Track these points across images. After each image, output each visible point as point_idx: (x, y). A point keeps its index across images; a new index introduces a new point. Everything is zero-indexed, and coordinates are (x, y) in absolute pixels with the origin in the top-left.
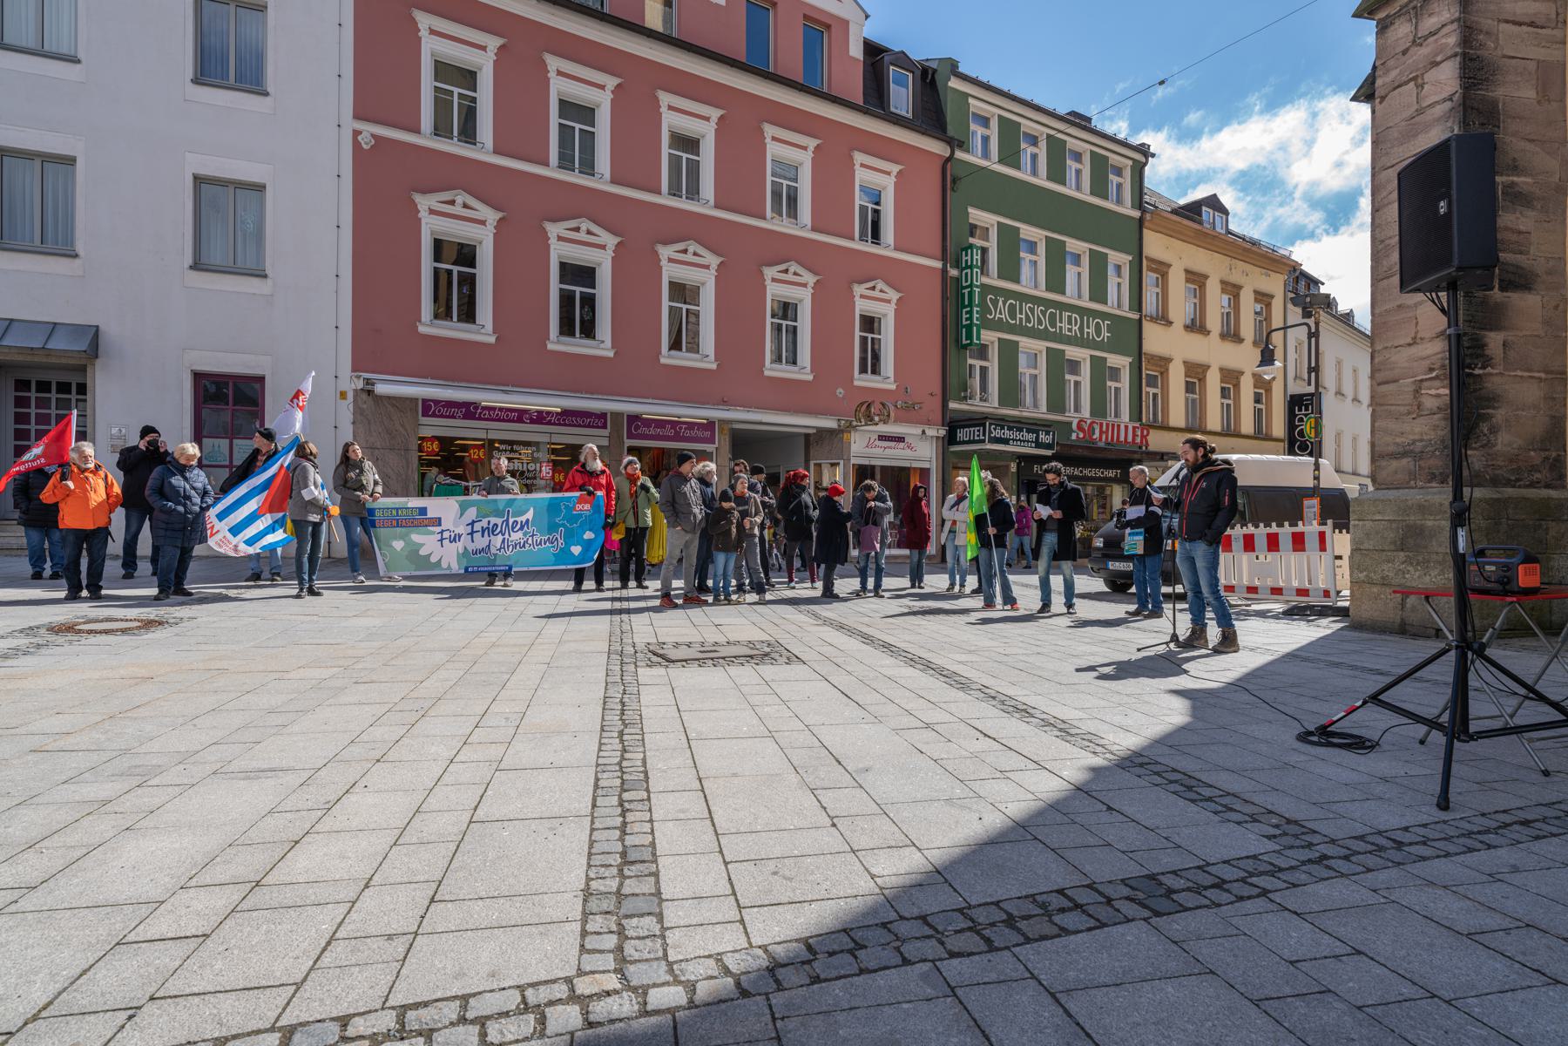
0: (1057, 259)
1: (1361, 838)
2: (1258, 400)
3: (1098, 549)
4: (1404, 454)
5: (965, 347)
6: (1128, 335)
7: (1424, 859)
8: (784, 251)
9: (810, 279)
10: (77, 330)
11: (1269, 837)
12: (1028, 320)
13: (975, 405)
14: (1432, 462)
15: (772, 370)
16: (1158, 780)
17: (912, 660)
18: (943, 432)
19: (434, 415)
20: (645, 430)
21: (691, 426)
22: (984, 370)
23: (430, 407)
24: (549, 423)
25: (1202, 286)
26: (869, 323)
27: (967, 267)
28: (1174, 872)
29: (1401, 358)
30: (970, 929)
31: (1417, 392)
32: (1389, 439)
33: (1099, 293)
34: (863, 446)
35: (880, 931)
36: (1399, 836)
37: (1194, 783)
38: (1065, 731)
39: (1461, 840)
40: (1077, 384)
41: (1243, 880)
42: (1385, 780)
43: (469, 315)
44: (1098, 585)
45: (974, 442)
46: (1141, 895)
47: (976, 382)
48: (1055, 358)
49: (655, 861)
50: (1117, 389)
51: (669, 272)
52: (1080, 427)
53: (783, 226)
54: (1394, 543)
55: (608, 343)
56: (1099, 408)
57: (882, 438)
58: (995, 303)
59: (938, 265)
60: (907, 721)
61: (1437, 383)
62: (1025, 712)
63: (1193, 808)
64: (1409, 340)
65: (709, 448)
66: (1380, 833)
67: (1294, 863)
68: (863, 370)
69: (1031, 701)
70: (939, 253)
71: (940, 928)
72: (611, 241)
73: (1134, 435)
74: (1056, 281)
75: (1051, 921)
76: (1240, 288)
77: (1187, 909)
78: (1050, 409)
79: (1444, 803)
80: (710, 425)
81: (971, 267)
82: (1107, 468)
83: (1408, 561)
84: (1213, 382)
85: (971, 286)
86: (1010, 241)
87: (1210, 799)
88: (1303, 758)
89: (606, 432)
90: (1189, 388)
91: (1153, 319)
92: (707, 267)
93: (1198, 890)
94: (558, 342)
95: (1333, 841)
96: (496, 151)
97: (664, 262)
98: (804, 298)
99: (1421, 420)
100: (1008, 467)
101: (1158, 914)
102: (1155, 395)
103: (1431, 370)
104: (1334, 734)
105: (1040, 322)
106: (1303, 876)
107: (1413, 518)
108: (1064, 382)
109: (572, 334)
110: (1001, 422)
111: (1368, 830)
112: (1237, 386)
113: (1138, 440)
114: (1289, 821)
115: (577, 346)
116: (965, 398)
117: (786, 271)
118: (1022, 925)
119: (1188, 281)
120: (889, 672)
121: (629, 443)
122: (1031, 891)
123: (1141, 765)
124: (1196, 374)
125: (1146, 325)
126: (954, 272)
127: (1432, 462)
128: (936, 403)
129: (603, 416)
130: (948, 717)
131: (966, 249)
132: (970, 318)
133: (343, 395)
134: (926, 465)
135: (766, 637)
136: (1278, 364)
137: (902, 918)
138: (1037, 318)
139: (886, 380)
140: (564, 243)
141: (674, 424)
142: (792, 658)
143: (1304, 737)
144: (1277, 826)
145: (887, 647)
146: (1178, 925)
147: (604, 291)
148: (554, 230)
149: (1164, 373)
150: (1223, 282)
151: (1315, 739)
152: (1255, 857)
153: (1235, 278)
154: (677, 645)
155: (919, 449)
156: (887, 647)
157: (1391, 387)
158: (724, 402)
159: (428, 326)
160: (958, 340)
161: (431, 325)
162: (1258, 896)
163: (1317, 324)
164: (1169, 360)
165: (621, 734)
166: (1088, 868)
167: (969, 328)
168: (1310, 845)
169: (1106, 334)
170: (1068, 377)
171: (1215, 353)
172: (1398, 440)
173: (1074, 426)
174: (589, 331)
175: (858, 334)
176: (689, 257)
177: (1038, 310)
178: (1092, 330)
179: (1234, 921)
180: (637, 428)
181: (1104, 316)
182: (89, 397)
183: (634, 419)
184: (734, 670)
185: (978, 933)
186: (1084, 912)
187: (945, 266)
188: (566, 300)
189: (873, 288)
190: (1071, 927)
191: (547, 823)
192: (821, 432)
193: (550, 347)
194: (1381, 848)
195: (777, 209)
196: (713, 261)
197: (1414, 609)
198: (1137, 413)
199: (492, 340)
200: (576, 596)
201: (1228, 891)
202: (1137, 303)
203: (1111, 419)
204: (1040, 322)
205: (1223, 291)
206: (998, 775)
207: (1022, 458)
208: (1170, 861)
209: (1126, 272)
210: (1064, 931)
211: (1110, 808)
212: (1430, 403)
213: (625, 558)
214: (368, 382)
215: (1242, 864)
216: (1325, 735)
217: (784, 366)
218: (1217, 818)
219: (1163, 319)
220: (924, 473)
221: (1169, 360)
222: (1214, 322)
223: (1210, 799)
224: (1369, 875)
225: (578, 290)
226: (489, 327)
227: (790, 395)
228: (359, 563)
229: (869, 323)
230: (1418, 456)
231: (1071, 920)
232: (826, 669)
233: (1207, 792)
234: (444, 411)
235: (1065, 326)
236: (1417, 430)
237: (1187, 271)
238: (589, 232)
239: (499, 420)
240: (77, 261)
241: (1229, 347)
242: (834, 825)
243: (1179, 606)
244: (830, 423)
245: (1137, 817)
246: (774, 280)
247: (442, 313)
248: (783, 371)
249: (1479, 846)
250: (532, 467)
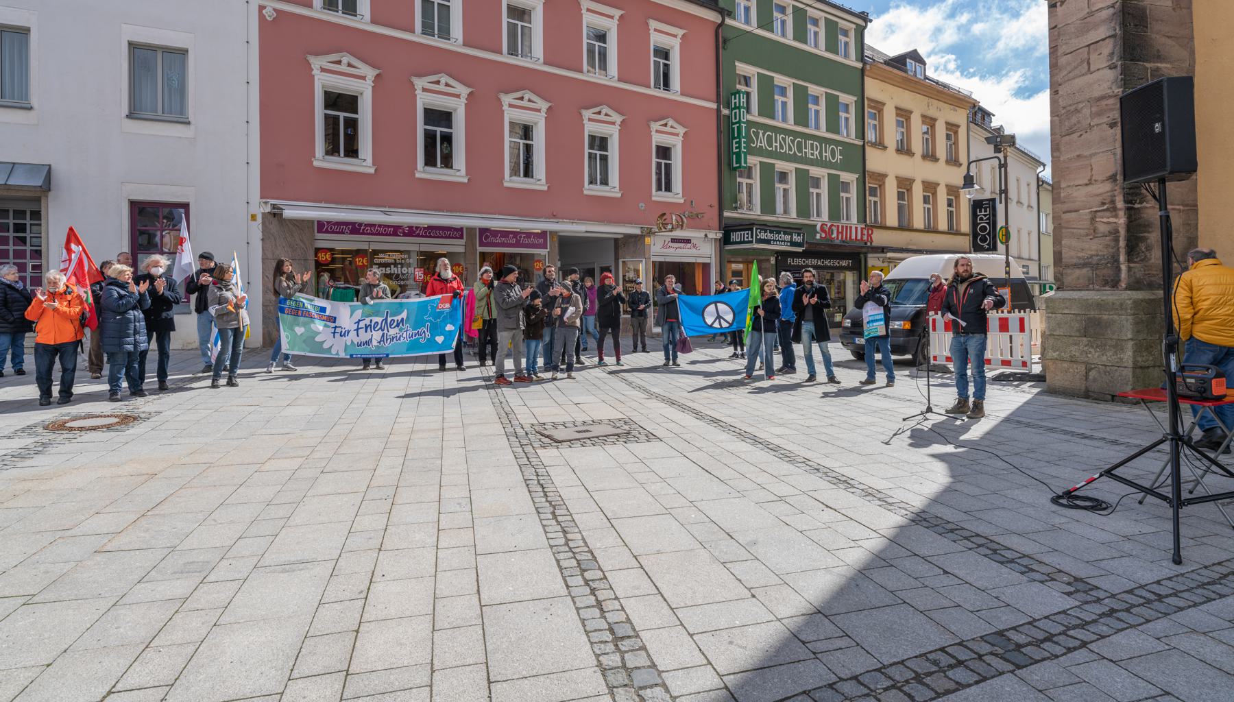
0: (802, 98)
1: (1130, 592)
2: (950, 205)
3: (847, 328)
4: (1084, 265)
5: (735, 169)
6: (855, 158)
7: (1181, 609)
8: (599, 97)
9: (617, 118)
10: (32, 168)
11: (1069, 594)
12: (781, 147)
13: (744, 214)
14: (1105, 271)
15: (589, 190)
16: (970, 545)
17: (742, 435)
18: (720, 235)
19: (327, 232)
20: (491, 239)
21: (529, 235)
22: (750, 186)
23: (322, 226)
24: (418, 236)
25: (908, 119)
26: (664, 152)
27: (736, 108)
28: (1014, 628)
30: (893, 687)
31: (1093, 219)
32: (1073, 253)
33: (833, 126)
34: (660, 248)
35: (830, 692)
36: (1156, 588)
37: (996, 547)
38: (885, 502)
39: (1200, 591)
40: (818, 195)
41: (1064, 633)
42: (1128, 538)
43: (352, 152)
44: (847, 355)
45: (744, 242)
46: (1000, 651)
47: (744, 196)
48: (802, 176)
49: (638, 636)
50: (848, 199)
51: (510, 115)
52: (822, 230)
53: (596, 77)
55: (463, 172)
56: (835, 213)
57: (674, 240)
58: (757, 134)
59: (714, 106)
60: (762, 495)
61: (1108, 214)
62: (845, 482)
63: (1004, 569)
65: (543, 252)
66: (1142, 587)
67: (1094, 617)
68: (659, 189)
69: (848, 472)
70: (714, 97)
71: (872, 687)
72: (464, 91)
73: (862, 234)
74: (802, 118)
75: (946, 676)
76: (935, 120)
77: (1037, 662)
78: (799, 214)
79: (1177, 560)
80: (543, 234)
81: (739, 108)
82: (842, 259)
84: (918, 192)
85: (739, 122)
86: (767, 87)
87: (1012, 561)
88: (1063, 520)
89: (462, 242)
90: (900, 196)
91: (874, 145)
92: (539, 111)
93: (1037, 643)
94: (424, 172)
95: (1113, 596)
96: (374, 21)
97: (505, 107)
98: (613, 133)
99: (1096, 240)
100: (768, 260)
101: (1019, 667)
102: (875, 203)
104: (1077, 498)
105: (790, 149)
106: (1105, 628)
107: (1093, 313)
108: (808, 194)
109: (435, 165)
110: (765, 226)
111: (1134, 585)
112: (934, 194)
113: (865, 238)
114: (1076, 579)
115: (438, 174)
116: (736, 208)
117: (599, 113)
118: (928, 680)
119: (897, 115)
120: (731, 447)
121: (480, 249)
122: (923, 651)
123: (952, 531)
124: (905, 185)
125: (868, 149)
126: (725, 112)
128: (715, 211)
129: (462, 229)
130: (792, 491)
131: (735, 94)
132: (739, 147)
133: (254, 217)
134: (707, 261)
135: (620, 416)
136: (976, 187)
137: (841, 679)
138: (789, 146)
139: (677, 194)
140: (427, 94)
141: (515, 234)
142: (651, 437)
143: (1056, 500)
144: (1069, 584)
145: (715, 421)
146: (1040, 674)
147: (459, 130)
148: (419, 83)
149: (882, 186)
150: (923, 116)
151: (1064, 501)
152: (1064, 612)
153: (932, 112)
154: (555, 425)
155: (702, 248)
156: (715, 421)
157: (1073, 215)
158: (554, 216)
159: (321, 159)
160: (730, 164)
161: (323, 160)
162: (1080, 647)
163: (1005, 158)
164: (886, 176)
165: (553, 513)
166: (953, 628)
167: (738, 155)
168: (1098, 600)
169: (838, 157)
170: (811, 190)
171: (918, 169)
172: (1080, 255)
173: (818, 228)
174: (447, 161)
175: (654, 160)
176: (525, 103)
177: (789, 139)
178: (828, 154)
179: (1073, 669)
180: (487, 237)
181: (837, 143)
182: (43, 222)
183: (483, 231)
184: (608, 447)
185: (899, 689)
186: (966, 667)
187: (719, 107)
188: (430, 138)
189: (666, 125)
190: (963, 682)
191: (542, 604)
192: (628, 238)
193: (418, 175)
194: (1149, 601)
195: (591, 63)
196: (543, 105)
198: (863, 217)
199: (372, 171)
200: (441, 374)
201: (1056, 643)
202: (861, 134)
203: (844, 221)
204: (790, 149)
205: (923, 123)
206: (853, 544)
207: (778, 253)
208: (1005, 620)
209: (852, 109)
210: (960, 686)
211: (945, 572)
212: (1102, 228)
213: (481, 343)
214: (274, 206)
215: (1058, 618)
216: (1069, 498)
217: (598, 187)
218: (1025, 578)
219: (880, 145)
220: (706, 267)
221: (886, 176)
222: (917, 146)
223: (1012, 561)
224: (1149, 625)
225: (439, 130)
226: (370, 161)
227: (604, 209)
228: (271, 350)
229: (664, 152)
230: (1095, 267)
231: (959, 674)
232: (682, 446)
233: (1009, 555)
234: (335, 228)
235: (809, 151)
237: (897, 108)
238: (447, 85)
239: (379, 234)
240: (31, 113)
241: (929, 165)
242: (753, 596)
243: (932, 381)
244: (635, 231)
245: (968, 579)
246: (590, 120)
247: (332, 150)
248: (598, 190)
249: (1213, 596)
250: (405, 270)
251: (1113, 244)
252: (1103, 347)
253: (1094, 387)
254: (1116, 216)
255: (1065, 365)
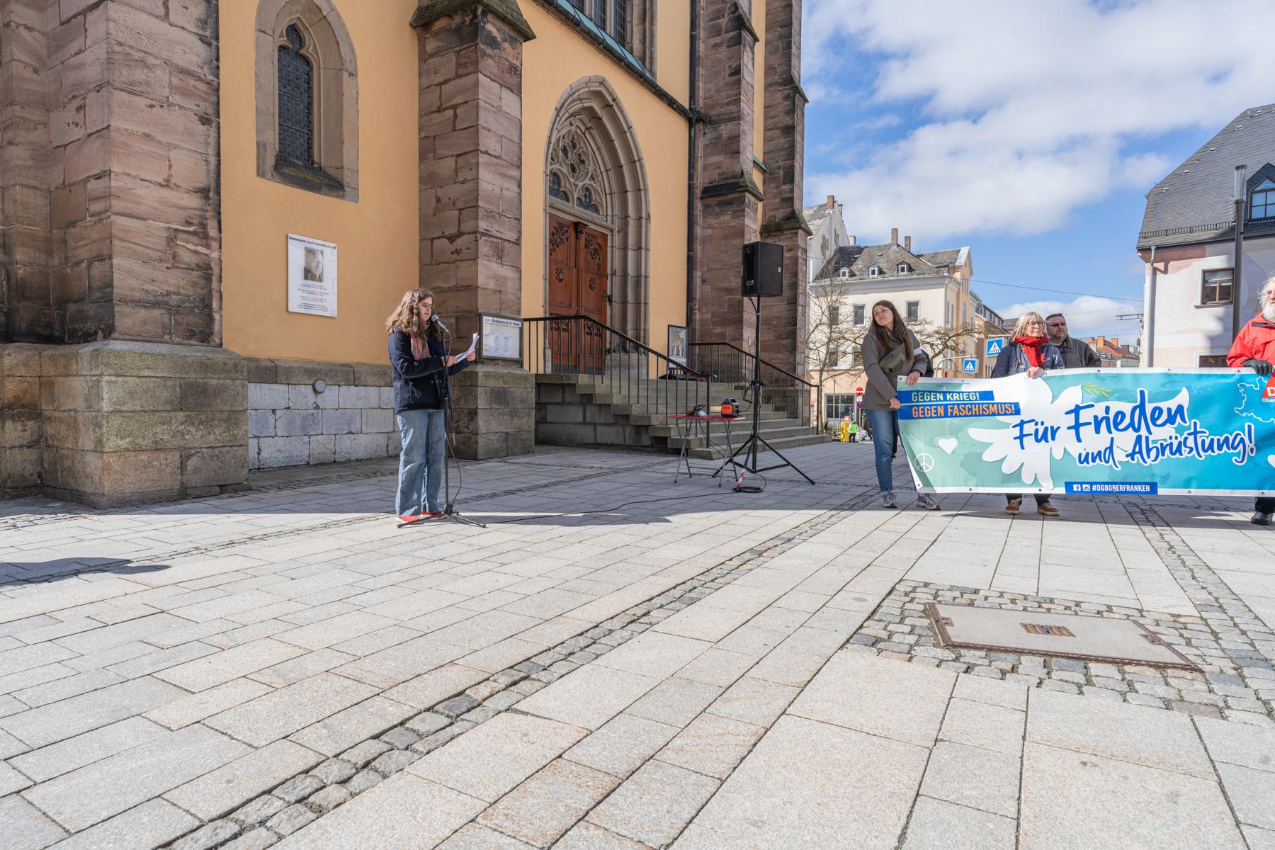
4: (156, 304)
14: (191, 318)
29: (150, 196)
31: (171, 240)
32: (135, 283)
54: (171, 402)
61: (196, 240)
64: (161, 180)
83: (189, 421)
103: (189, 223)
107: (193, 376)
127: (191, 318)
172: (146, 287)
197: (196, 470)
212: (186, 257)
230: (175, 310)
236: (173, 281)
251: (203, 282)
252: (209, 424)
253: (195, 480)
254: (208, 246)
255: (144, 457)
